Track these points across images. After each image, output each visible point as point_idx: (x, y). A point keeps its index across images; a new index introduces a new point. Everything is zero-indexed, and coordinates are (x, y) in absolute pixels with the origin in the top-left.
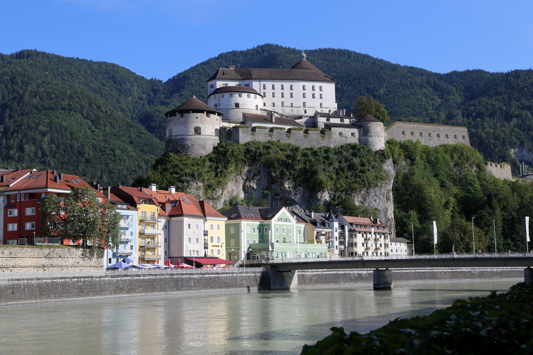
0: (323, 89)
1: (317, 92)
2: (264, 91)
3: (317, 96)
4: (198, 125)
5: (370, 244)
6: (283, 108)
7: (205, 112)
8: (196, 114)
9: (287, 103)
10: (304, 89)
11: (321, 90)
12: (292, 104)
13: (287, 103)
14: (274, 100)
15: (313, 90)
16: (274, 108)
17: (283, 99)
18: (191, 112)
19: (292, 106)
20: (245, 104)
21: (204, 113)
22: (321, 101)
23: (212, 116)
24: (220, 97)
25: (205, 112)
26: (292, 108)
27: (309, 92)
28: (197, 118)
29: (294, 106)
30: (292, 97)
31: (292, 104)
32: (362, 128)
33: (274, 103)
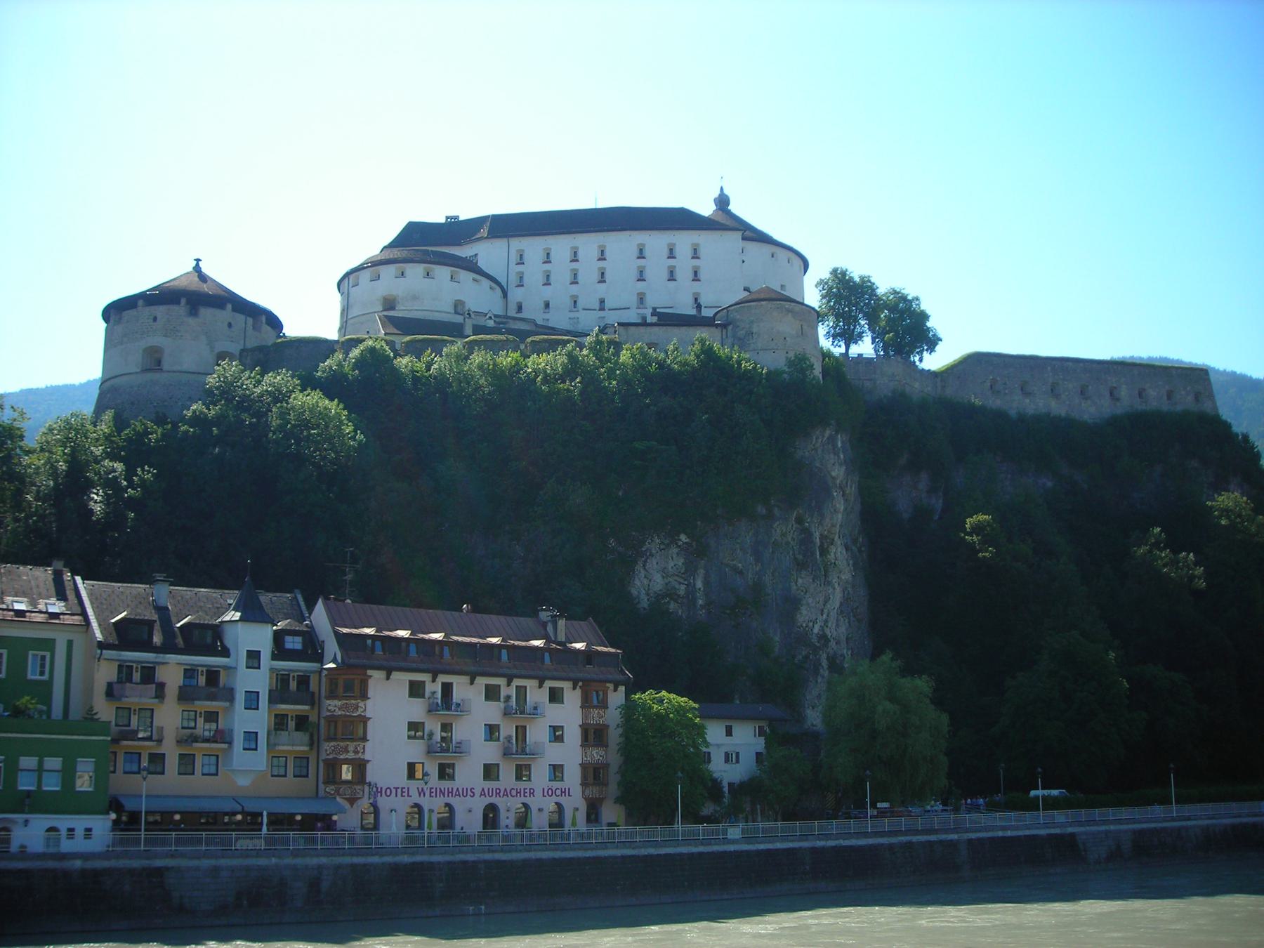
0: (703, 252)
1: (684, 264)
2: (520, 268)
3: (684, 274)
4: (156, 340)
5: (469, 730)
6: (572, 315)
7: (183, 301)
8: (153, 307)
9: (589, 297)
10: (641, 256)
11: (696, 256)
12: (602, 302)
13: (589, 297)
14: (547, 293)
15: (671, 256)
16: (547, 316)
17: (574, 289)
18: (140, 302)
19: (602, 309)
20: (415, 298)
21: (178, 303)
22: (696, 287)
23: (206, 313)
24: (351, 285)
25: (183, 301)
26: (602, 314)
27: (656, 266)
28: (155, 319)
29: (608, 305)
30: (602, 281)
31: (602, 302)
32: (730, 328)
33: (547, 305)
